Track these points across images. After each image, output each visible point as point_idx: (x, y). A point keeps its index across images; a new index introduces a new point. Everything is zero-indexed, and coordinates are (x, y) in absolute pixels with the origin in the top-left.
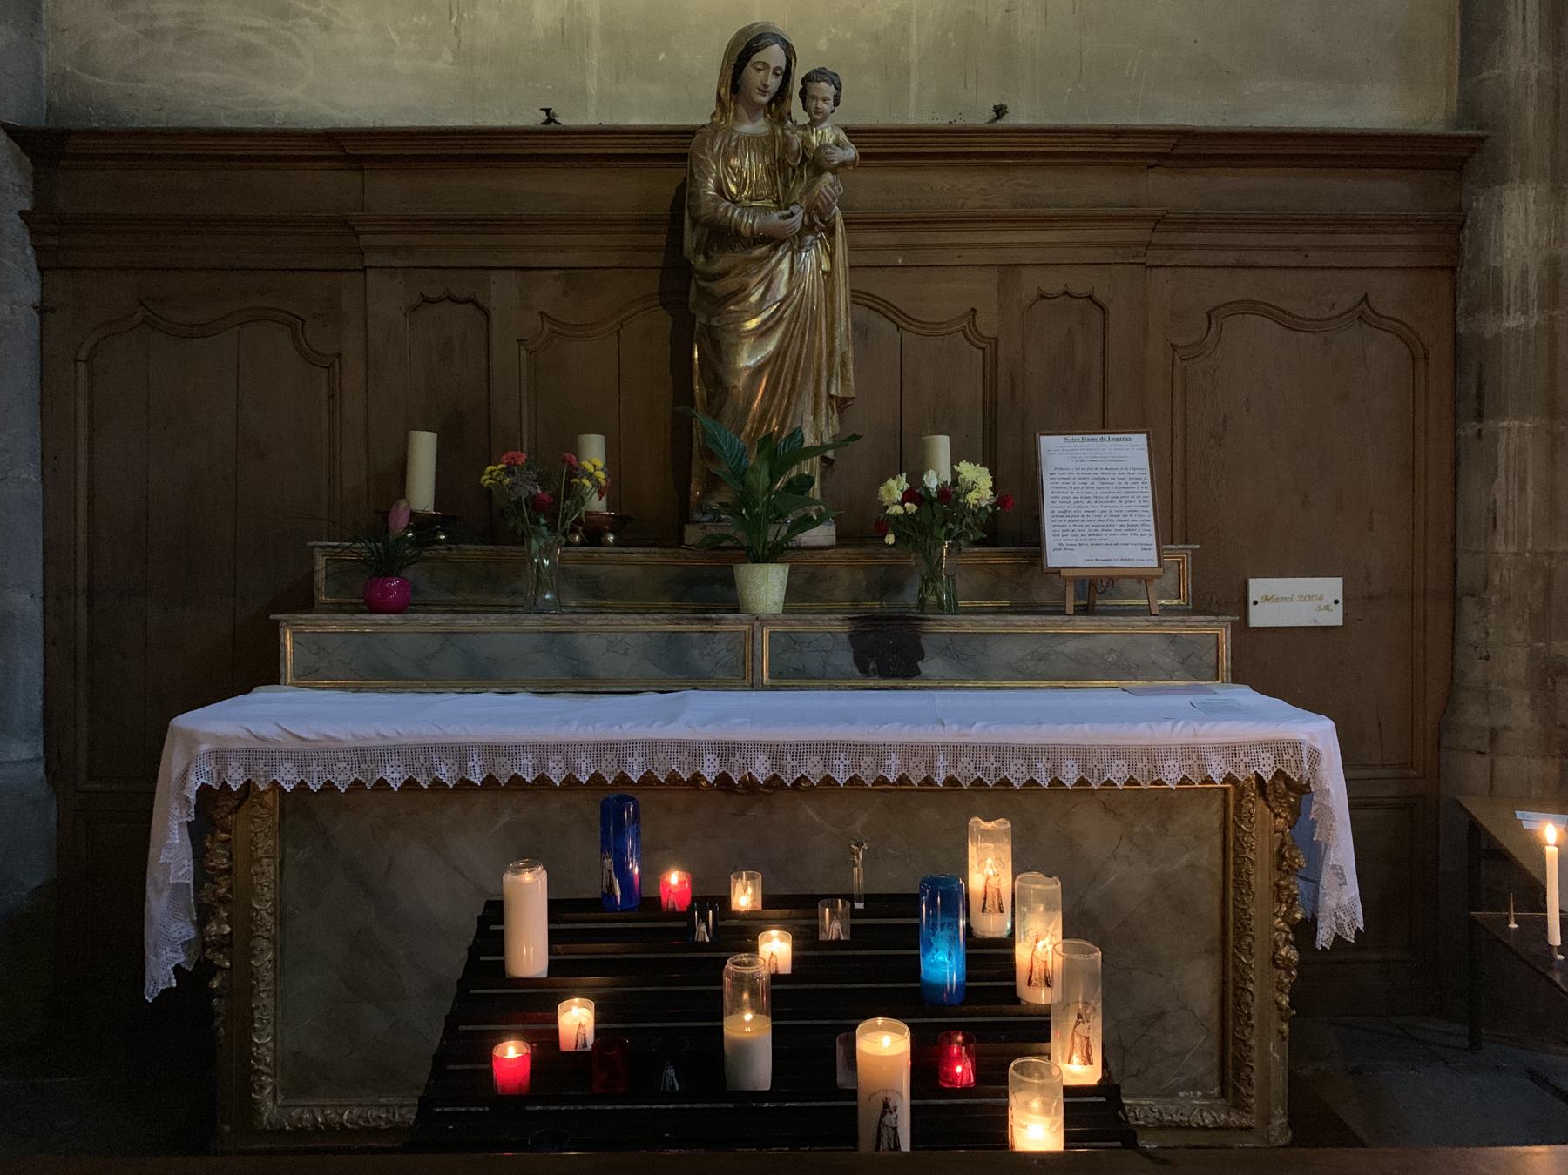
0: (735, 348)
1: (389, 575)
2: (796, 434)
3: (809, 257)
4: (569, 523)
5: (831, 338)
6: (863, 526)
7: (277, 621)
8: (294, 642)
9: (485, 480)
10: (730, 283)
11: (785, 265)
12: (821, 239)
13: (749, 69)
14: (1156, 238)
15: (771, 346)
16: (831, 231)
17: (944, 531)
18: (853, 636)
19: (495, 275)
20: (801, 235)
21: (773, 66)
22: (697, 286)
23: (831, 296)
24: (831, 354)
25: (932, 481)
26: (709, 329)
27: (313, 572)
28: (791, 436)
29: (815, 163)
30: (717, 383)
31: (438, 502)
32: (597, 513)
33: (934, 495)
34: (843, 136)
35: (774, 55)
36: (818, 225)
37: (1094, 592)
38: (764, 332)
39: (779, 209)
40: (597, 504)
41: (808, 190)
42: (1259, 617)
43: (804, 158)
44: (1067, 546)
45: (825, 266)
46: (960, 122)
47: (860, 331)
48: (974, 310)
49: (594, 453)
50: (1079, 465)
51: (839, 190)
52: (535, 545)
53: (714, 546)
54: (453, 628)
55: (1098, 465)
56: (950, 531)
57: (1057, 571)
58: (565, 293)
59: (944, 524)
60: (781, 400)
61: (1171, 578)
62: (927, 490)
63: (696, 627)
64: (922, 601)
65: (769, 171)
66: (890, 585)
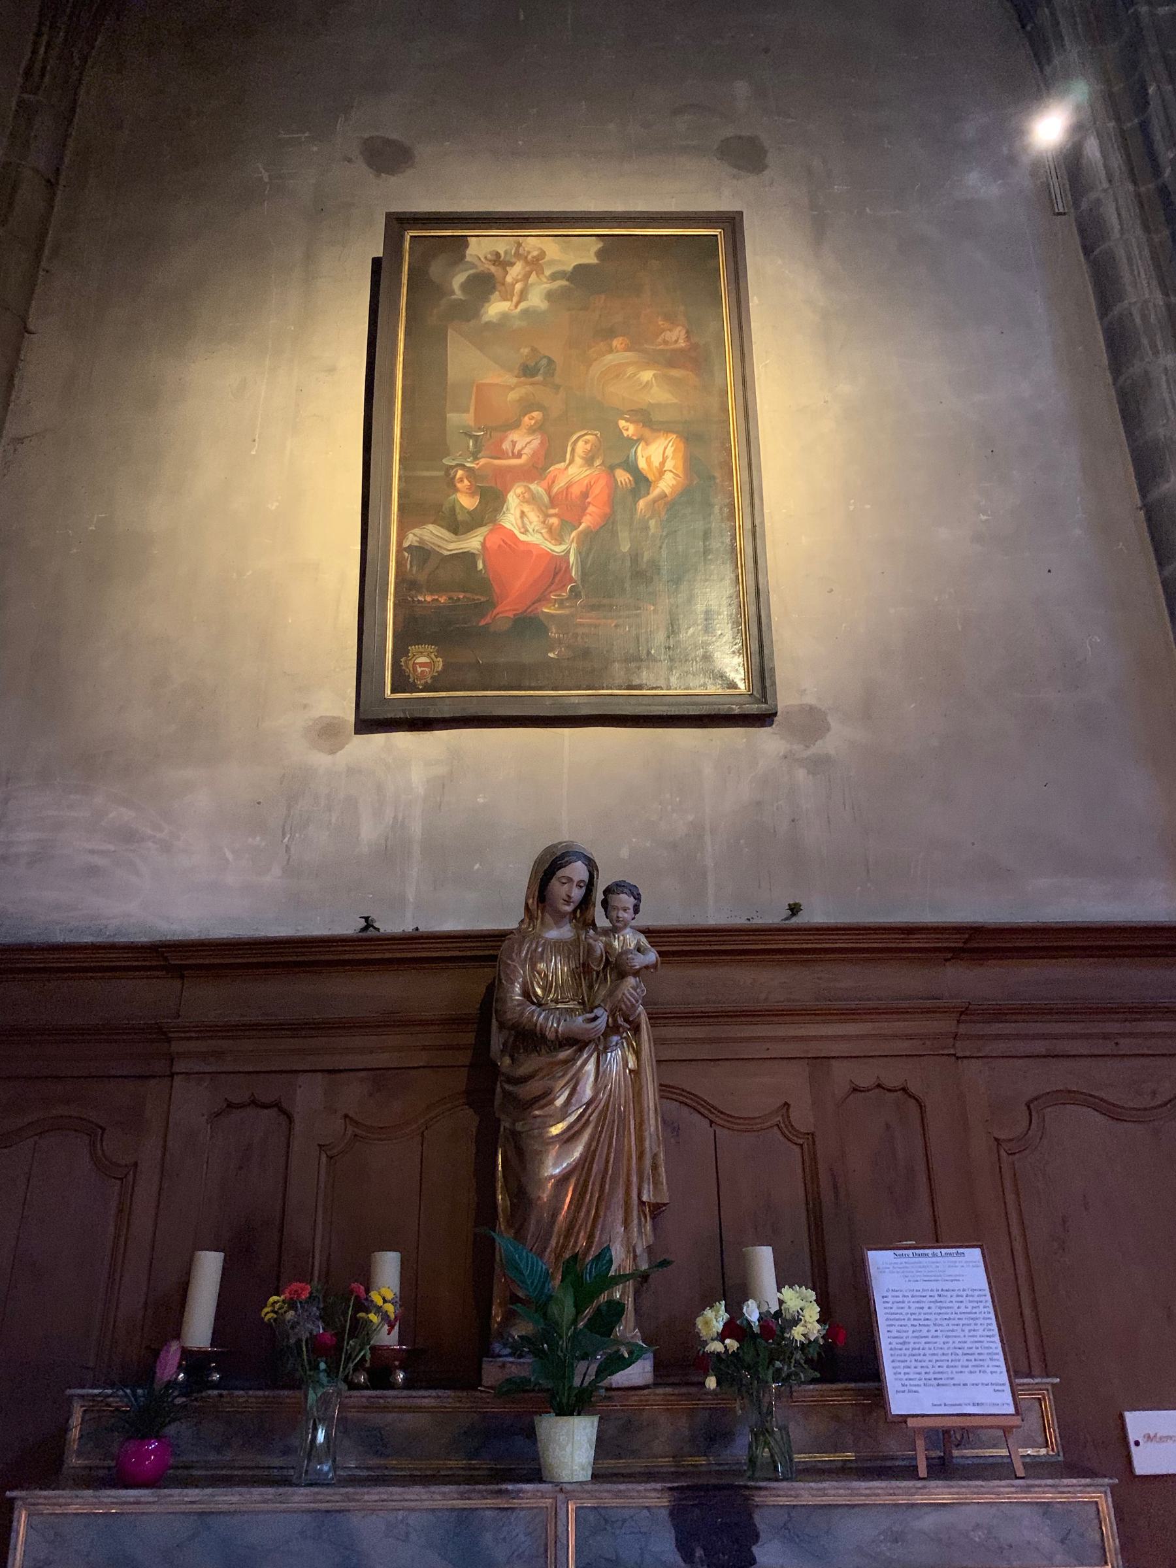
0: (539, 1155)
1: (146, 1437)
2: (604, 1257)
3: (614, 1057)
4: (351, 1365)
5: (640, 1139)
6: (680, 1361)
7: (12, 1500)
8: (29, 1526)
9: (267, 1314)
10: (534, 1088)
11: (591, 1067)
12: (627, 1038)
13: (554, 883)
14: (962, 1029)
15: (577, 1152)
16: (636, 1029)
17: (771, 1371)
18: (677, 1513)
19: (302, 1078)
20: (606, 1035)
21: (576, 879)
22: (503, 1090)
23: (638, 1094)
24: (641, 1157)
25: (752, 1312)
26: (515, 1135)
27: (66, 1430)
28: (598, 1257)
29: (617, 967)
30: (521, 1198)
31: (217, 1335)
32: (388, 1348)
33: (756, 1330)
34: (644, 940)
35: (578, 870)
36: (623, 1024)
37: (949, 1450)
38: (568, 1138)
39: (585, 1011)
40: (388, 1338)
41: (611, 993)
42: (1146, 1462)
43: (608, 962)
44: (911, 1393)
45: (632, 1064)
46: (759, 921)
47: (670, 1126)
48: (786, 1103)
49: (388, 1272)
50: (913, 1286)
51: (643, 990)
52: (312, 1397)
53: (515, 1388)
54: (212, 1507)
55: (934, 1285)
56: (779, 1370)
57: (904, 1418)
58: (371, 1095)
59: (771, 1362)
60: (588, 1212)
61: (1033, 1420)
62: (749, 1322)
63: (489, 1502)
64: (752, 1461)
65: (573, 973)
66: (715, 1435)
